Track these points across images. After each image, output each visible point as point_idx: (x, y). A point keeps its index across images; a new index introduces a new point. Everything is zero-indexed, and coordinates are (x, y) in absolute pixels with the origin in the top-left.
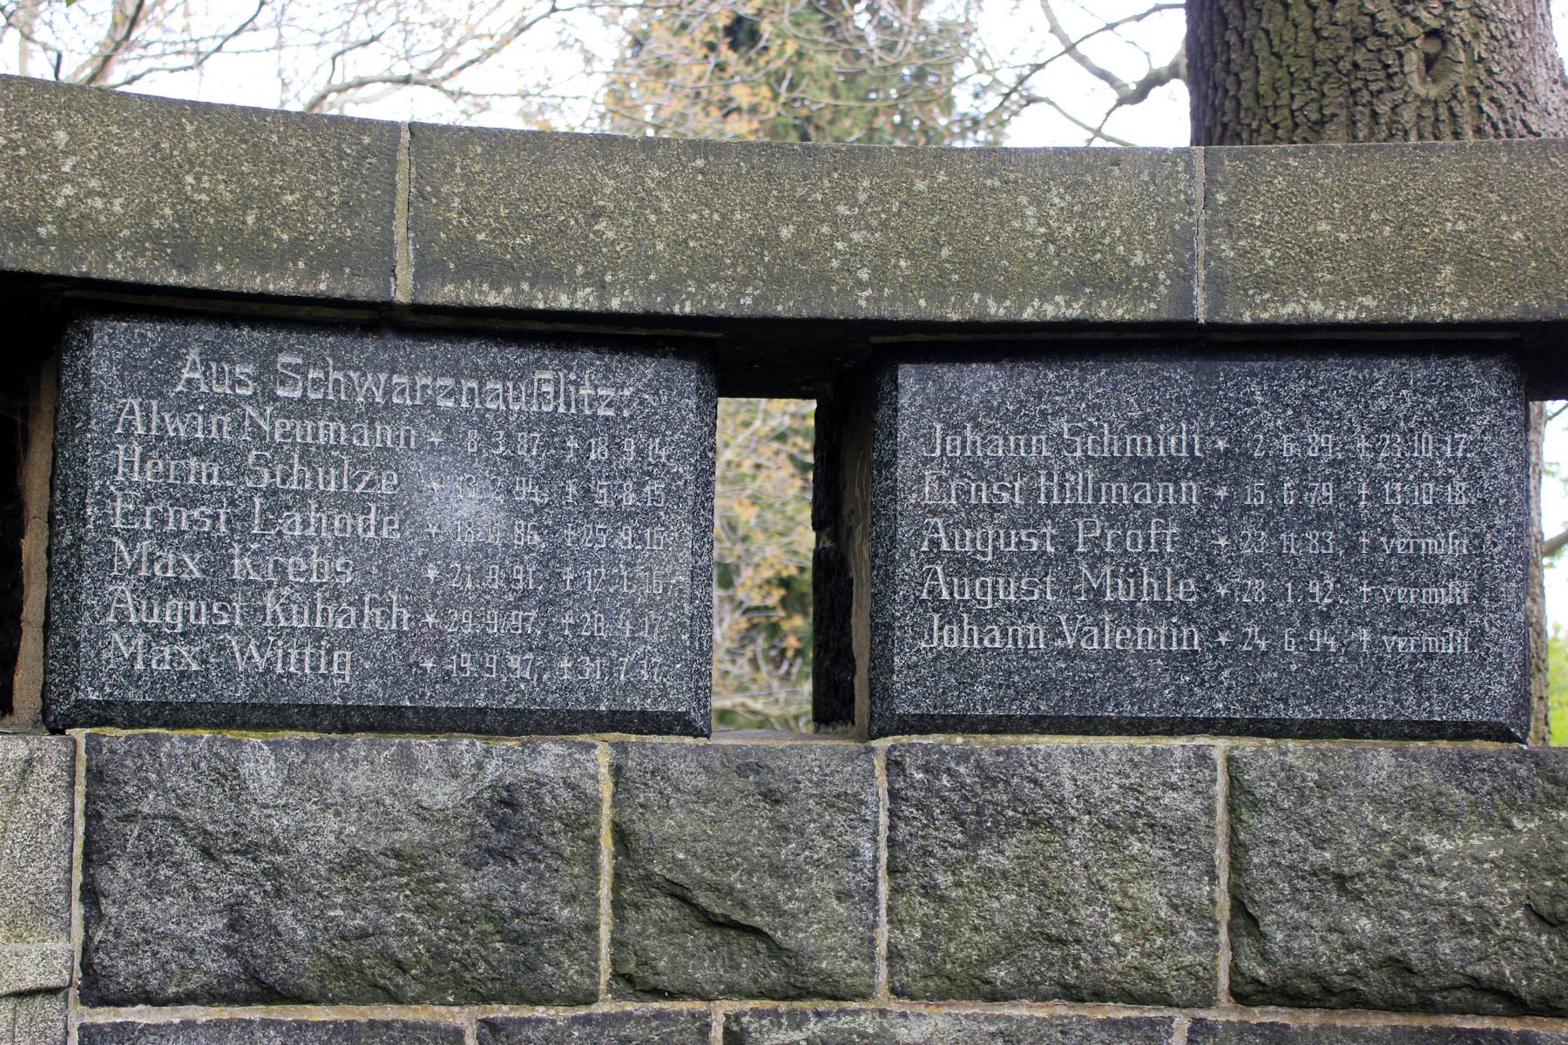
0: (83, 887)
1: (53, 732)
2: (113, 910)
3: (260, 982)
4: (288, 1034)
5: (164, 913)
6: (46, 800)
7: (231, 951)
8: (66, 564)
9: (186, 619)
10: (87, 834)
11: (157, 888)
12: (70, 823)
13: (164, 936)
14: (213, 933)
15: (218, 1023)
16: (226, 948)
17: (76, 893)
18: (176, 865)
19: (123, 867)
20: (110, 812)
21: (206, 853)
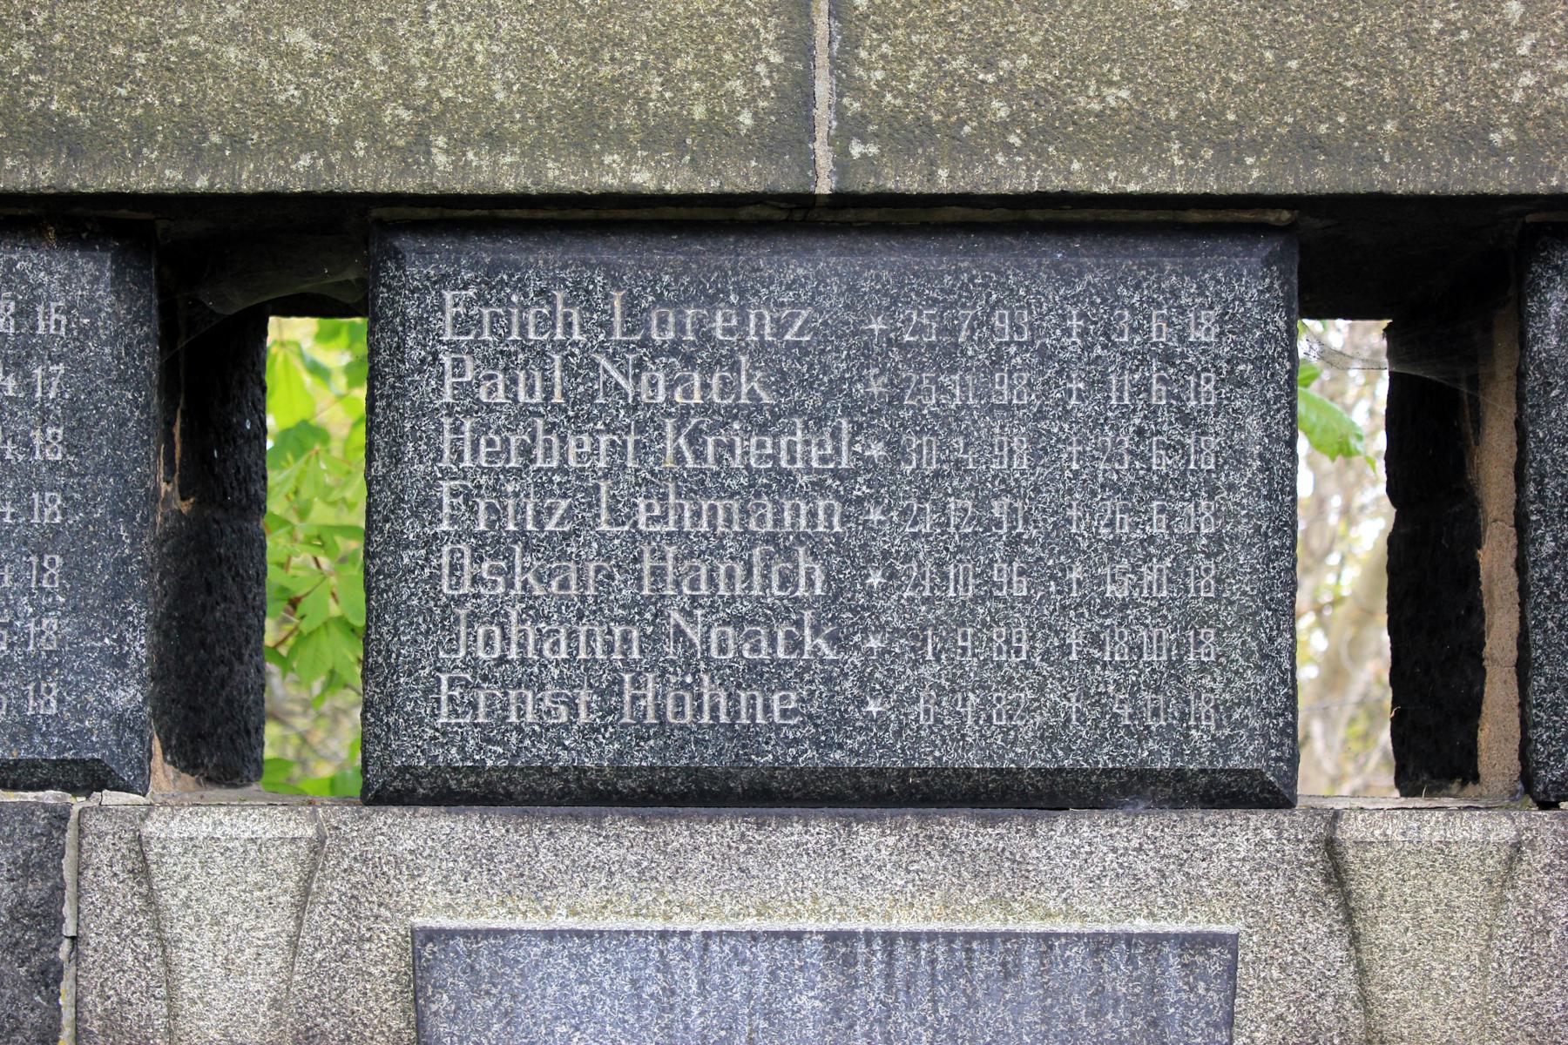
1: (1545, 805)
6: (1541, 897)
8: (1548, 580)
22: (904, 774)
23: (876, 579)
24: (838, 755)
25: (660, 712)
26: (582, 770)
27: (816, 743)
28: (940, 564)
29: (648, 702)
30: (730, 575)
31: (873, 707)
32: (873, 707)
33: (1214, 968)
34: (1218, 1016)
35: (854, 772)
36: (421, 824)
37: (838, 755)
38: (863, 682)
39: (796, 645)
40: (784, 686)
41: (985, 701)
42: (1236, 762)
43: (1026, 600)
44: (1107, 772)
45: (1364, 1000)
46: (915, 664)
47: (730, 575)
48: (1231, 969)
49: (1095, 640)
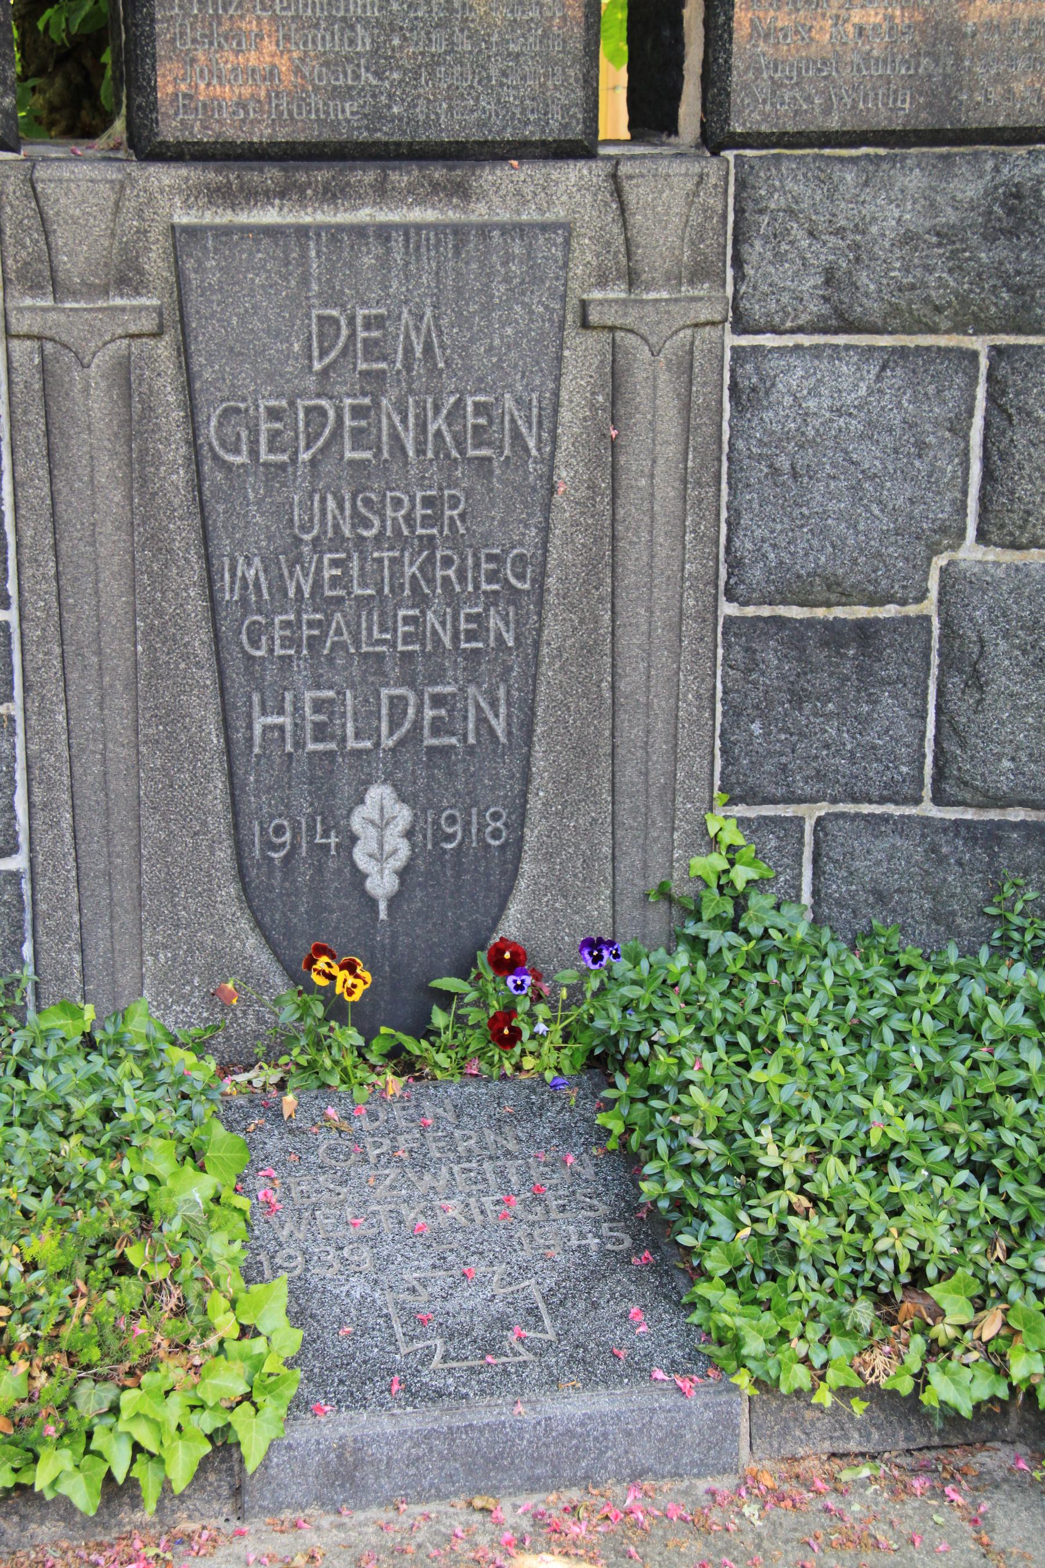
0: (733, 258)
2: (752, 272)
3: (845, 320)
4: (862, 354)
5: (782, 274)
7: (826, 299)
8: (721, 37)
9: (799, 73)
10: (736, 222)
11: (779, 257)
12: (724, 216)
13: (784, 289)
14: (815, 287)
15: (816, 347)
16: (823, 297)
17: (729, 262)
18: (791, 243)
19: (758, 244)
20: (750, 206)
21: (811, 234)
22: (411, 144)
23: (396, 42)
24: (379, 135)
25: (290, 113)
26: (252, 143)
27: (367, 128)
28: (428, 33)
29: (284, 107)
30: (323, 38)
31: (395, 110)
32: (395, 110)
33: (560, 240)
34: (561, 263)
35: (386, 144)
36: (173, 172)
37: (379, 135)
38: (390, 96)
39: (357, 77)
40: (352, 98)
41: (450, 107)
42: (570, 136)
43: (470, 52)
44: (508, 142)
45: (629, 255)
46: (415, 87)
47: (323, 38)
48: (567, 242)
49: (504, 74)
